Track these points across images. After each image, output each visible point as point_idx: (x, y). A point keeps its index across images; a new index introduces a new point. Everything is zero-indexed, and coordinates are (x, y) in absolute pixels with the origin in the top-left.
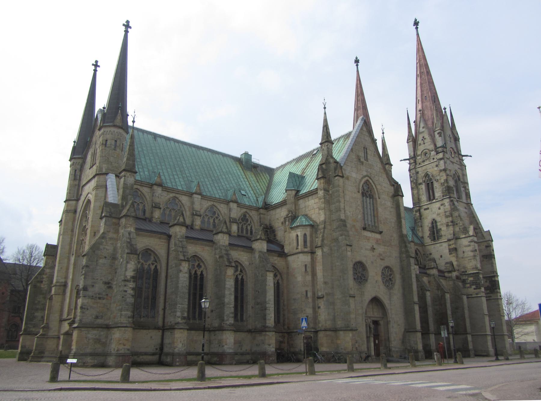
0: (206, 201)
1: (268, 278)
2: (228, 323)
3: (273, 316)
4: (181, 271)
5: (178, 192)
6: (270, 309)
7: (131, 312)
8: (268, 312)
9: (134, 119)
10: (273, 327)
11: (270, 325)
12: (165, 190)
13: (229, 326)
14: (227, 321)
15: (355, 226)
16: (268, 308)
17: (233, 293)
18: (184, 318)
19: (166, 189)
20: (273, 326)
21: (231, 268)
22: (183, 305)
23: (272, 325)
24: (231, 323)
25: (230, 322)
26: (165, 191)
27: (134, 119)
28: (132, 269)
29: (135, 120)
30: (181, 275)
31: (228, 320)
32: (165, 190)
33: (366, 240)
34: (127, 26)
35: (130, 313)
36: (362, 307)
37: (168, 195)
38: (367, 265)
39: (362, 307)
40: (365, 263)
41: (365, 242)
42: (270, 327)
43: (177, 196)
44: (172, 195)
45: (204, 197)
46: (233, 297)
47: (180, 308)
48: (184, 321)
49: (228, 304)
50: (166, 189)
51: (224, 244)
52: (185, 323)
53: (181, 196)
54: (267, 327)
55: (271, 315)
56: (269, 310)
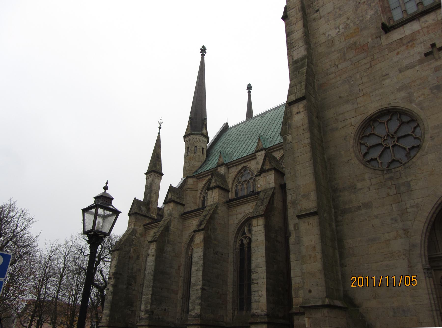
0: (278, 152)
1: (255, 229)
2: (194, 314)
3: (264, 293)
4: (149, 255)
5: (244, 160)
6: (260, 281)
7: (109, 310)
8: (254, 287)
9: (160, 126)
10: (265, 315)
11: (259, 312)
12: (232, 165)
13: (195, 318)
14: (192, 311)
15: (355, 43)
16: (254, 281)
17: (201, 268)
18: (147, 312)
19: (233, 164)
20: (263, 313)
21: (199, 233)
22: (147, 295)
23: (262, 311)
24: (196, 313)
25: (196, 311)
26: (234, 166)
27: (160, 126)
28: (114, 266)
29: (161, 126)
30: (149, 259)
31: (193, 309)
32: (232, 165)
33: (403, 48)
34: (203, 50)
35: (108, 311)
36: (406, 231)
37: (237, 169)
38: (414, 107)
39: (406, 231)
40: (402, 104)
41: (398, 53)
42: (258, 316)
43: (246, 164)
44: (240, 167)
45: (273, 149)
46: (200, 274)
47: (145, 300)
48: (147, 316)
49: (194, 285)
50: (233, 164)
51: (212, 203)
52: (147, 318)
53: (249, 162)
54: (254, 315)
55: (260, 293)
56: (257, 283)
